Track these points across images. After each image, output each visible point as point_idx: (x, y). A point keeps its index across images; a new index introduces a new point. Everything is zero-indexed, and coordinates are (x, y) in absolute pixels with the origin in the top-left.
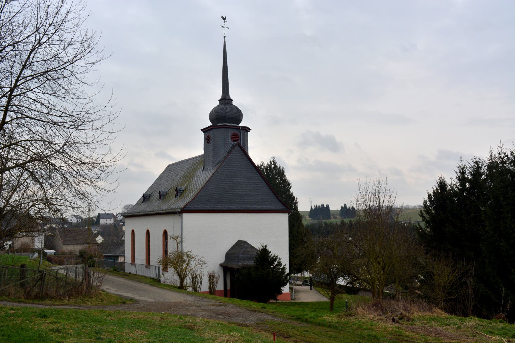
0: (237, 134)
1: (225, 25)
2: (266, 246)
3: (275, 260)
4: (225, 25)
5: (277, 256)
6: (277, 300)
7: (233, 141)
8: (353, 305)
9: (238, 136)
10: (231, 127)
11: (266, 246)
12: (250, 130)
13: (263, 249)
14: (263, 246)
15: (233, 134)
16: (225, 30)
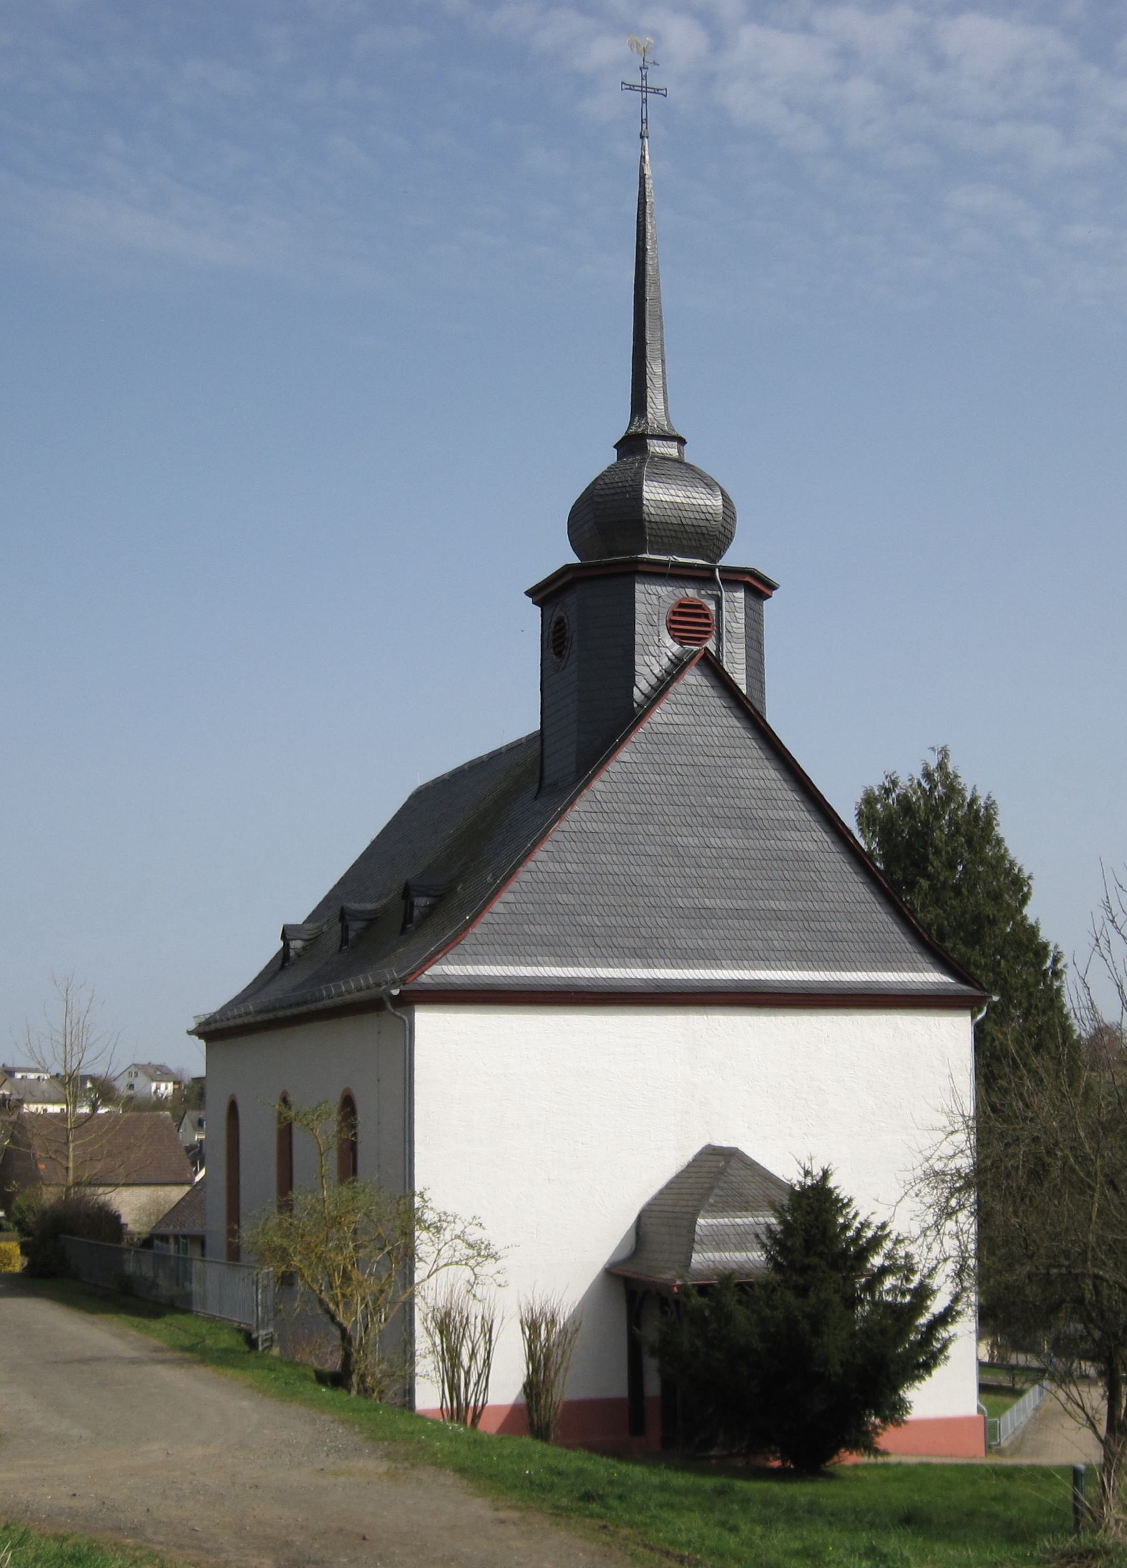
0: (700, 607)
1: (644, 78)
2: (826, 1174)
3: (876, 1243)
4: (644, 78)
5: (883, 1226)
6: (877, 1452)
7: (680, 640)
8: (299, 1309)
9: (706, 616)
10: (669, 570)
11: (826, 1174)
12: (772, 587)
13: (812, 1187)
14: (807, 1173)
15: (681, 605)
16: (644, 101)
